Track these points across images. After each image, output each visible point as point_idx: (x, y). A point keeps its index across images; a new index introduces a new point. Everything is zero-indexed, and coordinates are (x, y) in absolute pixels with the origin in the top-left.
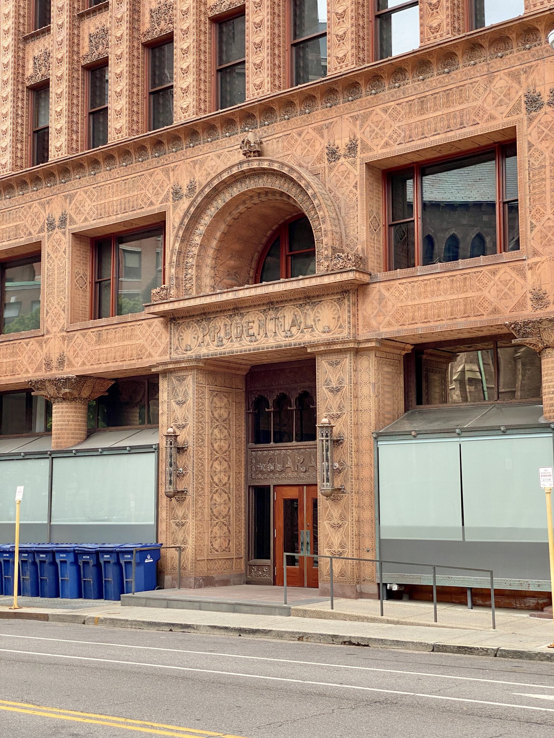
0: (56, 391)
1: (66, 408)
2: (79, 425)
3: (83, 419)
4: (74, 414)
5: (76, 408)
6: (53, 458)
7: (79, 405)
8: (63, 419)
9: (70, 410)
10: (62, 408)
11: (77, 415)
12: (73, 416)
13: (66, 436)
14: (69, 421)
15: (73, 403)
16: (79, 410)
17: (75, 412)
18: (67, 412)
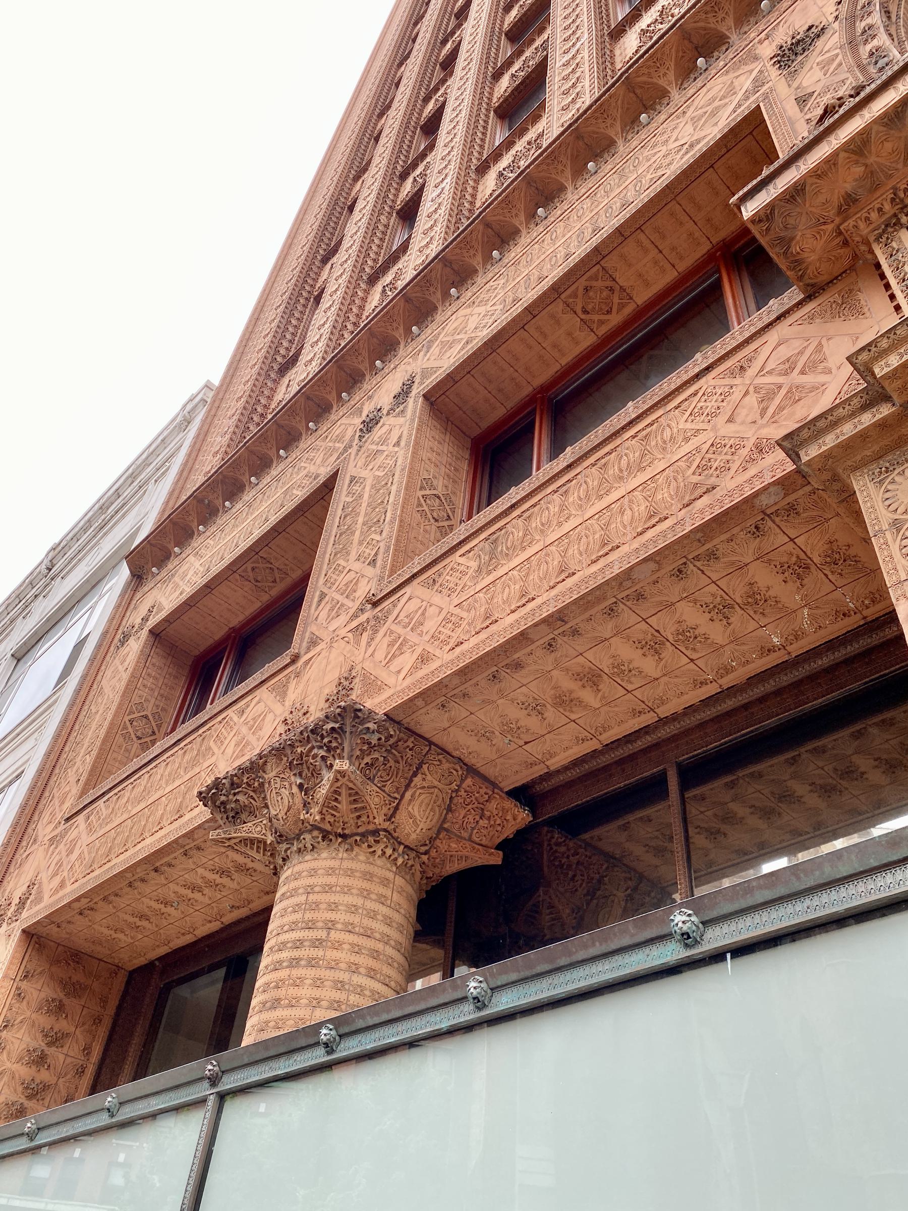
0: (299, 797)
1: (330, 872)
2: (375, 954)
3: (395, 935)
4: (359, 901)
5: (368, 876)
6: (222, 1097)
7: (382, 868)
8: (309, 915)
9: (343, 881)
10: (313, 873)
11: (370, 905)
12: (353, 909)
13: (306, 992)
14: (330, 926)
15: (361, 853)
16: (382, 890)
17: (365, 894)
18: (328, 889)
